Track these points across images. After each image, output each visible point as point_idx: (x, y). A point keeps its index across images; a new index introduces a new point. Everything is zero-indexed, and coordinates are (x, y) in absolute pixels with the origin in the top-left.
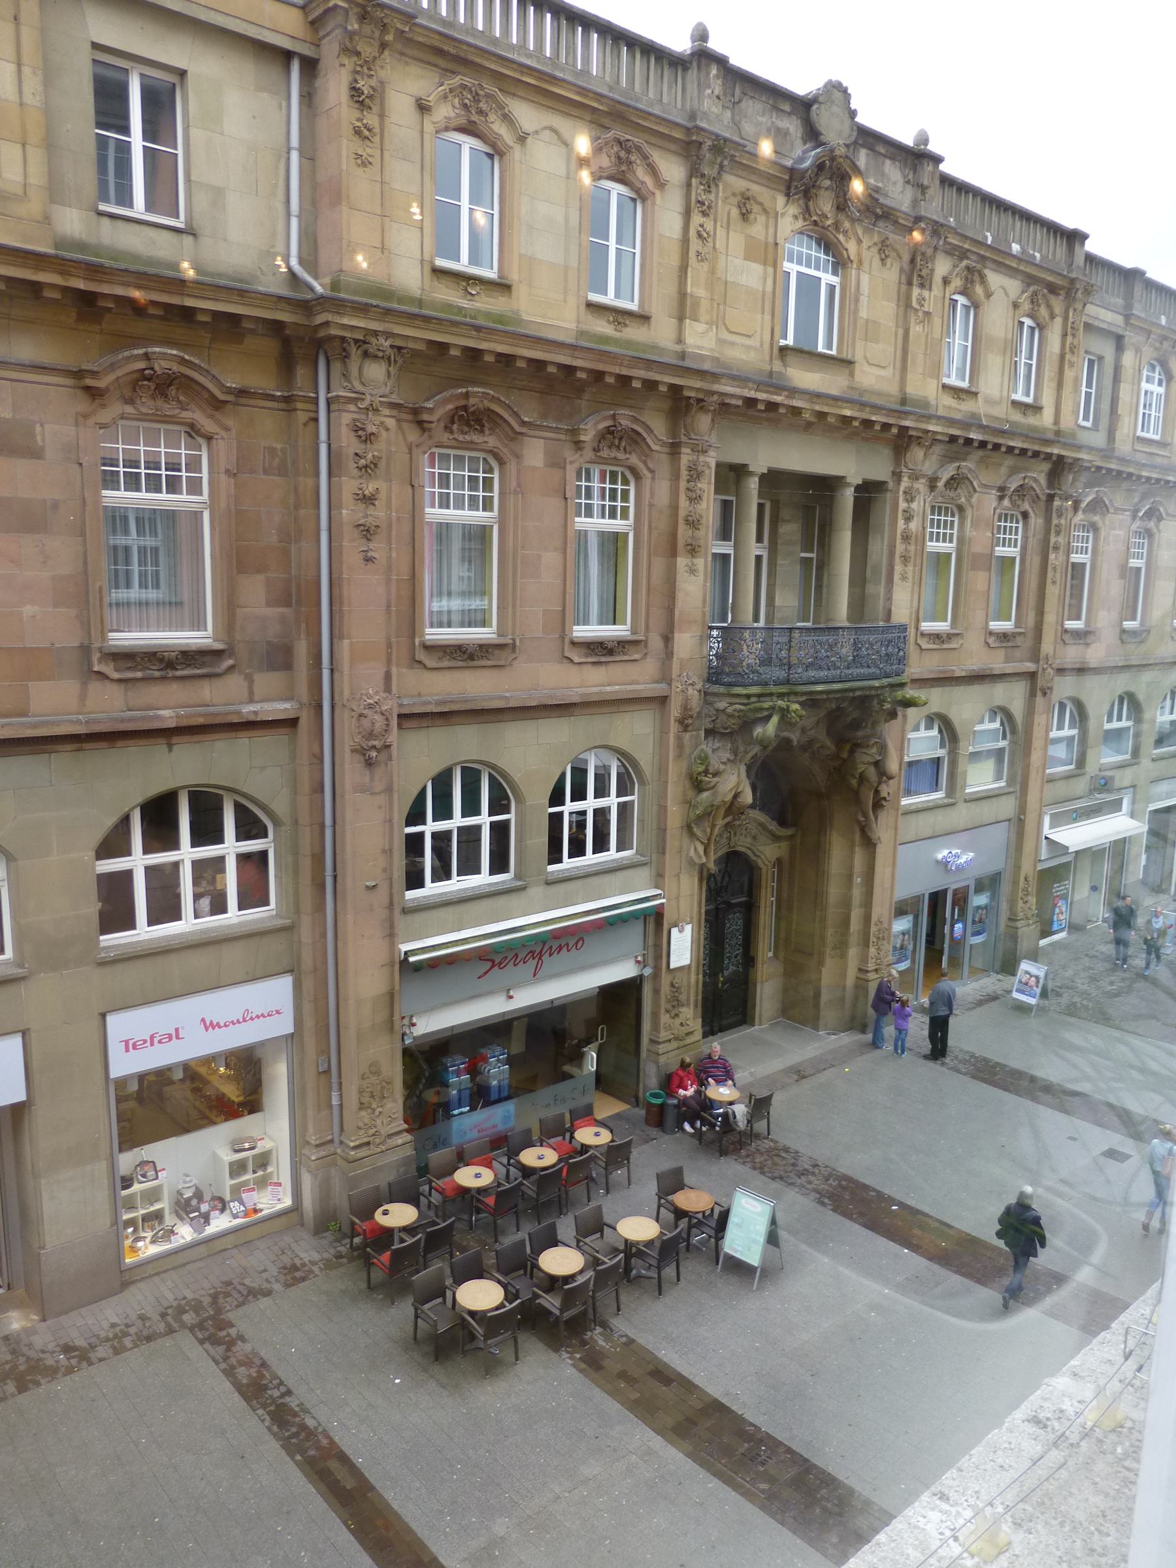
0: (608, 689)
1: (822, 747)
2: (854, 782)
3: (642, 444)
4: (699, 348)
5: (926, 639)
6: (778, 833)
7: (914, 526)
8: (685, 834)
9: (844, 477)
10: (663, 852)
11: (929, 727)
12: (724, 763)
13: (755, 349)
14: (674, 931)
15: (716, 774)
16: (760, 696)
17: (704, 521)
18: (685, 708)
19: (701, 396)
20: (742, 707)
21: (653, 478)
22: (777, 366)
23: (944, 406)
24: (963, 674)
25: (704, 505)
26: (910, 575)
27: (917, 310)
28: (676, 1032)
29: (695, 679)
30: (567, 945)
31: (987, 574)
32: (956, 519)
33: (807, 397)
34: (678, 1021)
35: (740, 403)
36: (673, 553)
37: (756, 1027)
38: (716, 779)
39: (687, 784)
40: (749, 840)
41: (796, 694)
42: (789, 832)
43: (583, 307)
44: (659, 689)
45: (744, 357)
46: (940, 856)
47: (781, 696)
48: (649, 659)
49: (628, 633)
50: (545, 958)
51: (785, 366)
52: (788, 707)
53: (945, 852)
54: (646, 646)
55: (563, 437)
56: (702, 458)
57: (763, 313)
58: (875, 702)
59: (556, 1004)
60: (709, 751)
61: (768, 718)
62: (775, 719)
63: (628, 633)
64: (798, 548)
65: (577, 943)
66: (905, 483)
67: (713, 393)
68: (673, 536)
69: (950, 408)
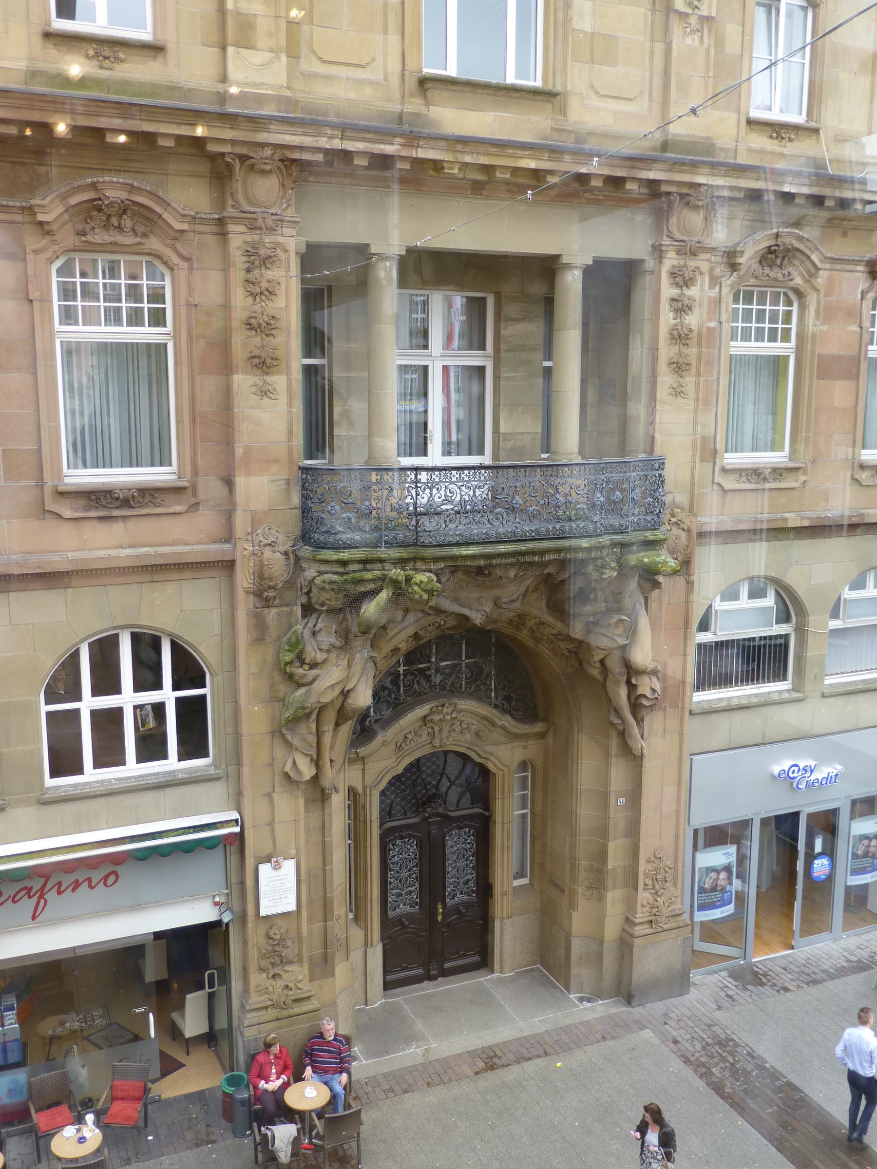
0: (114, 552)
1: (542, 624)
2: (595, 672)
3: (160, 222)
4: (255, 85)
5: (733, 477)
6: (514, 730)
7: (692, 320)
8: (278, 742)
9: (558, 256)
10: (239, 764)
11: (755, 594)
12: (328, 651)
13: (372, 83)
14: (265, 870)
15: (314, 665)
16: (365, 562)
17: (282, 324)
18: (260, 575)
19: (243, 151)
20: (335, 577)
21: (191, 269)
22: (414, 105)
23: (751, 151)
24: (806, 523)
25: (281, 302)
26: (690, 389)
27: (686, 15)
28: (275, 997)
29: (281, 538)
30: (89, 880)
31: (853, 384)
32: (795, 309)
33: (444, 144)
34: (280, 983)
35: (319, 157)
36: (227, 368)
37: (496, 975)
38: (313, 673)
39: (277, 677)
40: (468, 737)
41: (423, 559)
42: (538, 728)
43: (37, 40)
44: (217, 551)
45: (352, 95)
46: (776, 769)
47: (401, 562)
48: (202, 510)
49: (174, 477)
50: (52, 896)
51: (427, 104)
52: (408, 579)
53: (786, 764)
54: (195, 493)
55: (18, 218)
56: (268, 239)
57: (386, 32)
58: (591, 568)
59: (79, 953)
60: (307, 634)
61: (374, 593)
62: (384, 595)
63: (174, 477)
64: (540, 355)
65: (106, 878)
66: (671, 260)
67: (263, 145)
68: (225, 345)
69: (761, 152)
